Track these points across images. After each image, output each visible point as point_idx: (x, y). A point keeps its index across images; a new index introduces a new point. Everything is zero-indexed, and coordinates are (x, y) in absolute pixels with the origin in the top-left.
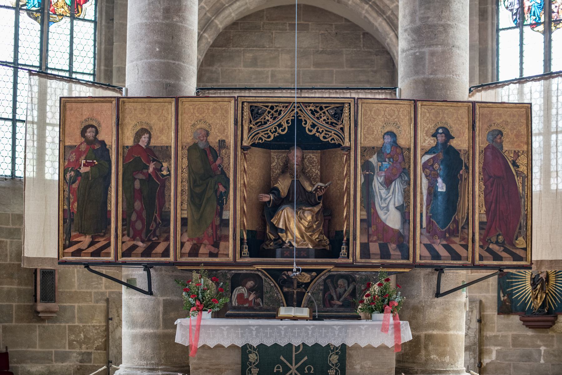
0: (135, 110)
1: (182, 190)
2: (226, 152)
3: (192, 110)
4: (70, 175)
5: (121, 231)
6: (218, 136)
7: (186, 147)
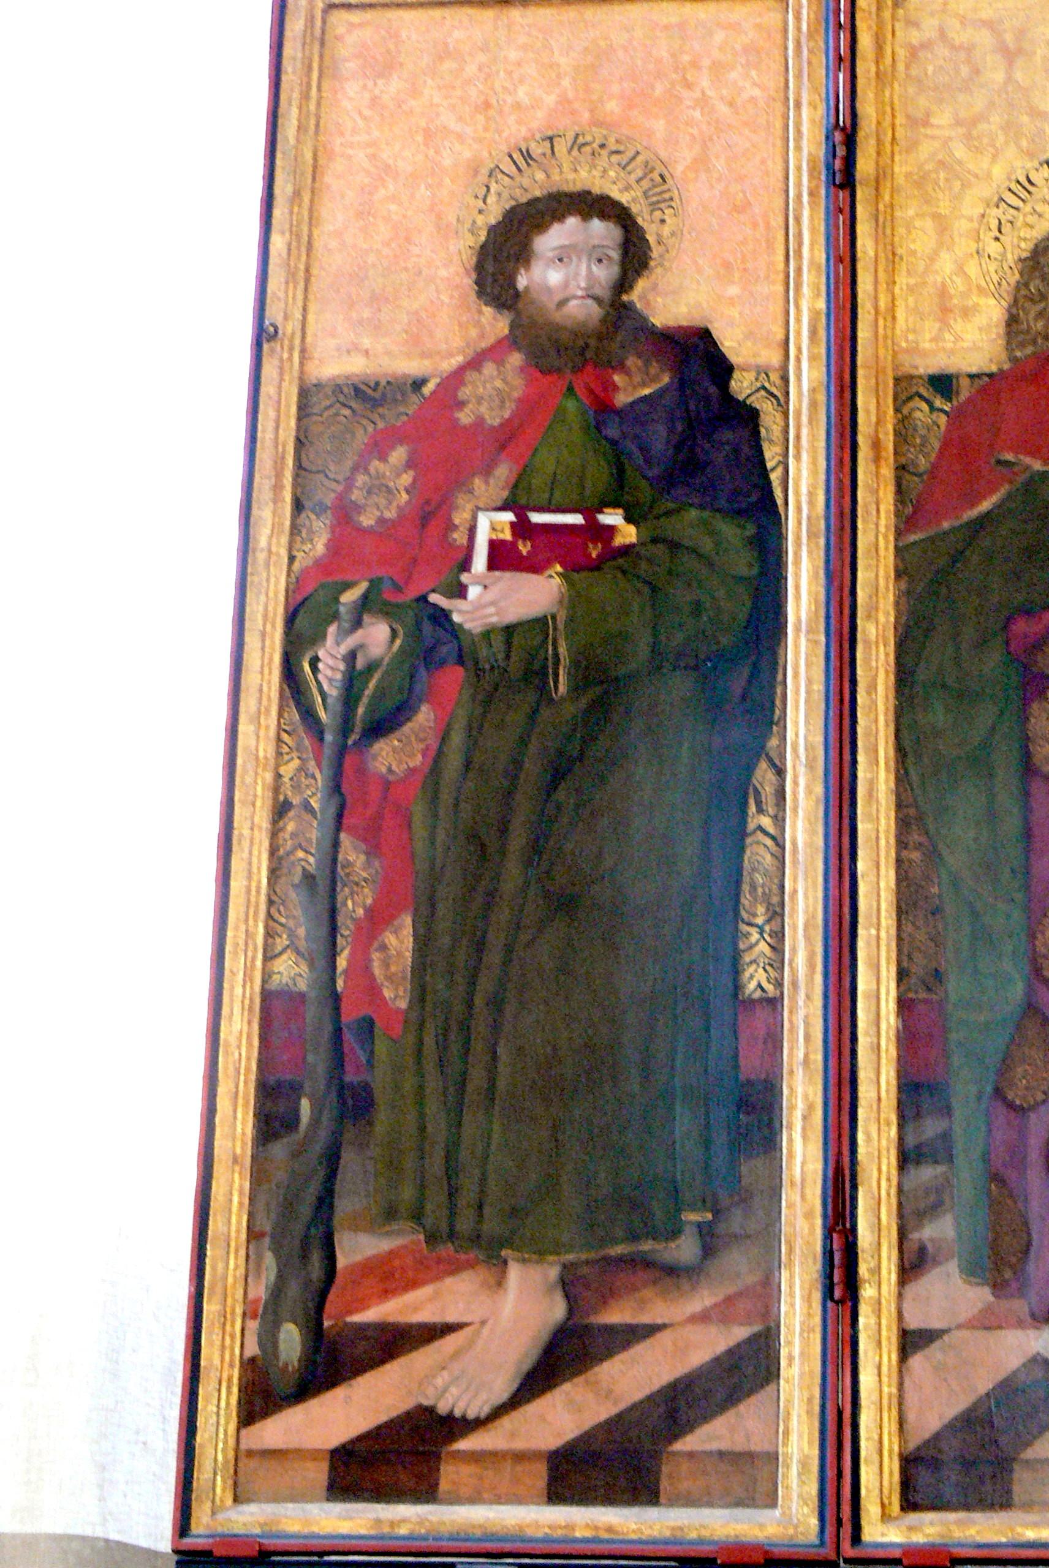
4: (351, 657)
5: (888, 1217)
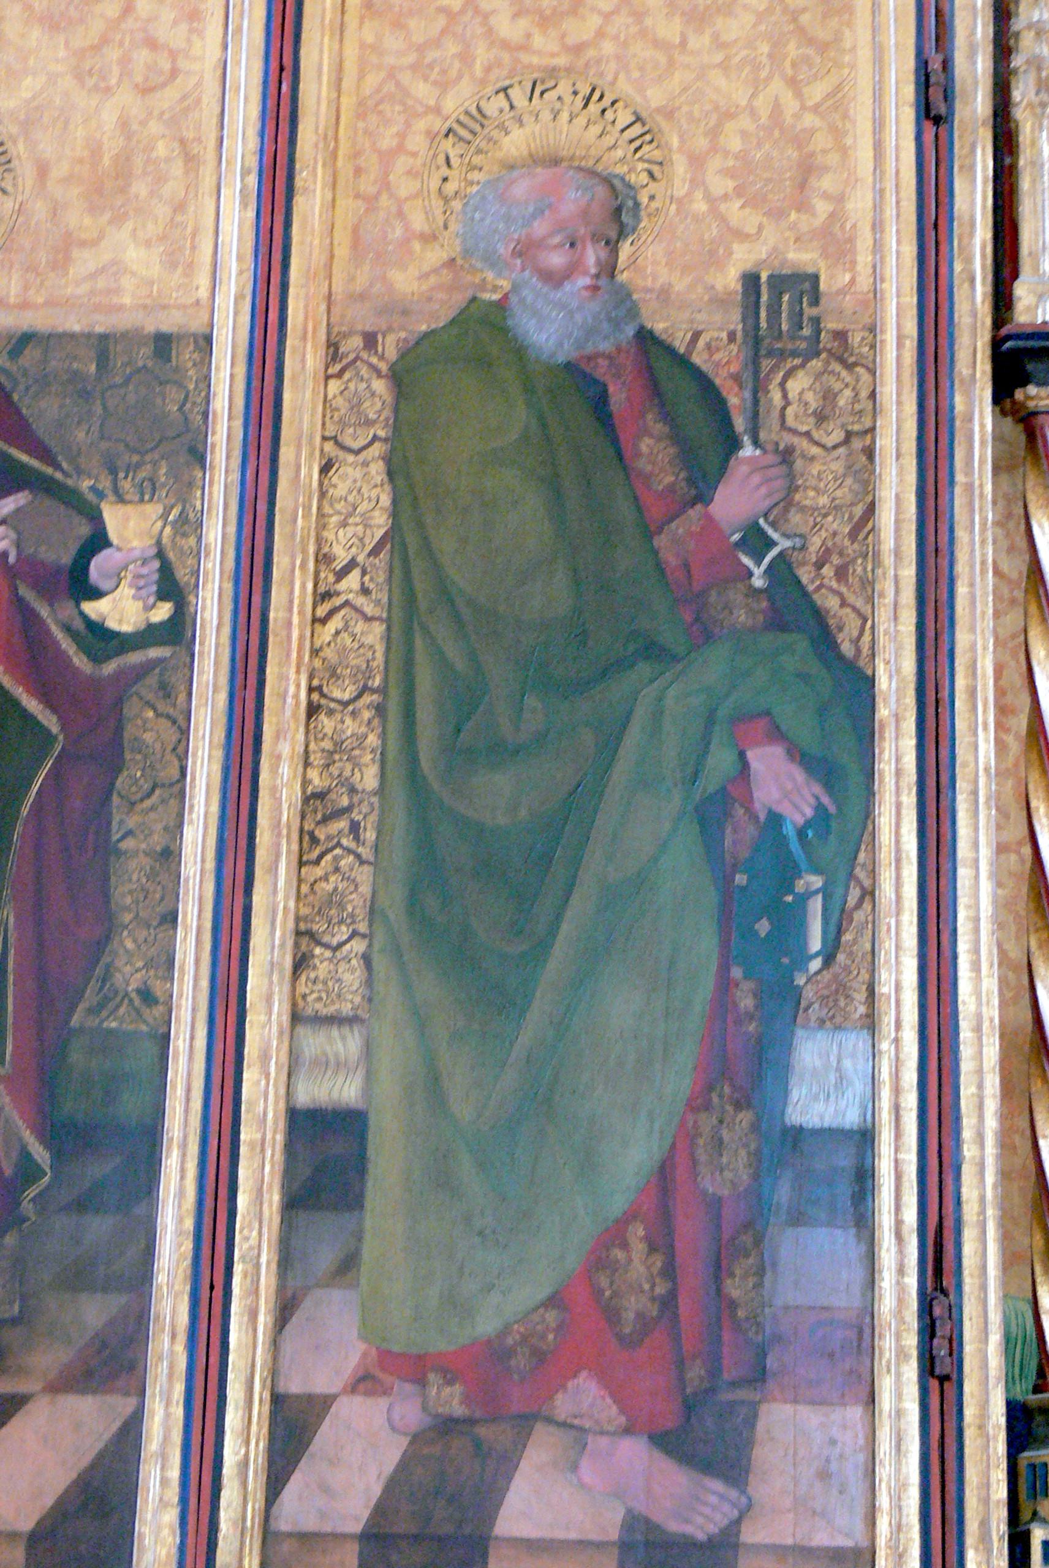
1: (313, 798)
2: (829, 396)
6: (741, 236)
7: (370, 340)
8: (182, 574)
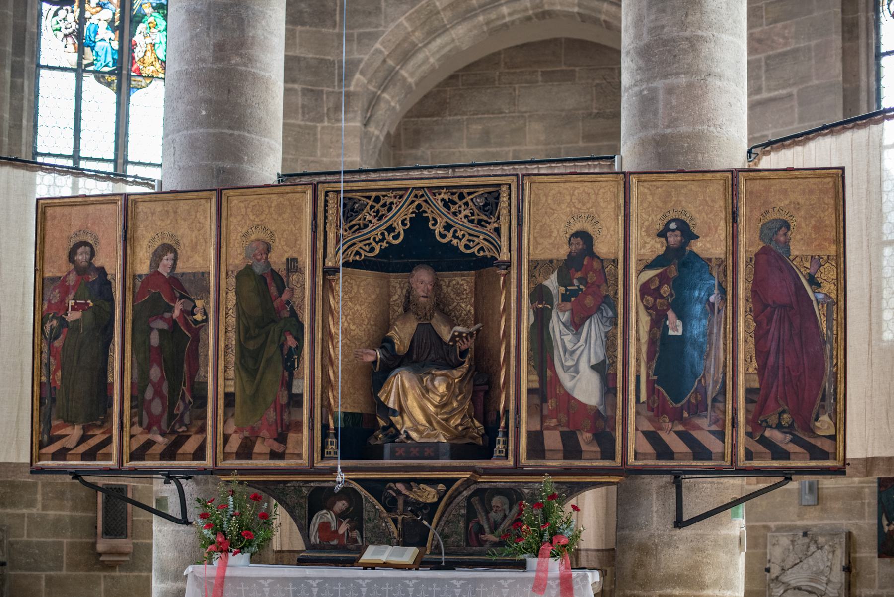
0: (153, 214)
1: (226, 346)
3: (243, 210)
5: (128, 417)
6: (286, 252)
7: (233, 272)
8: (207, 311)
